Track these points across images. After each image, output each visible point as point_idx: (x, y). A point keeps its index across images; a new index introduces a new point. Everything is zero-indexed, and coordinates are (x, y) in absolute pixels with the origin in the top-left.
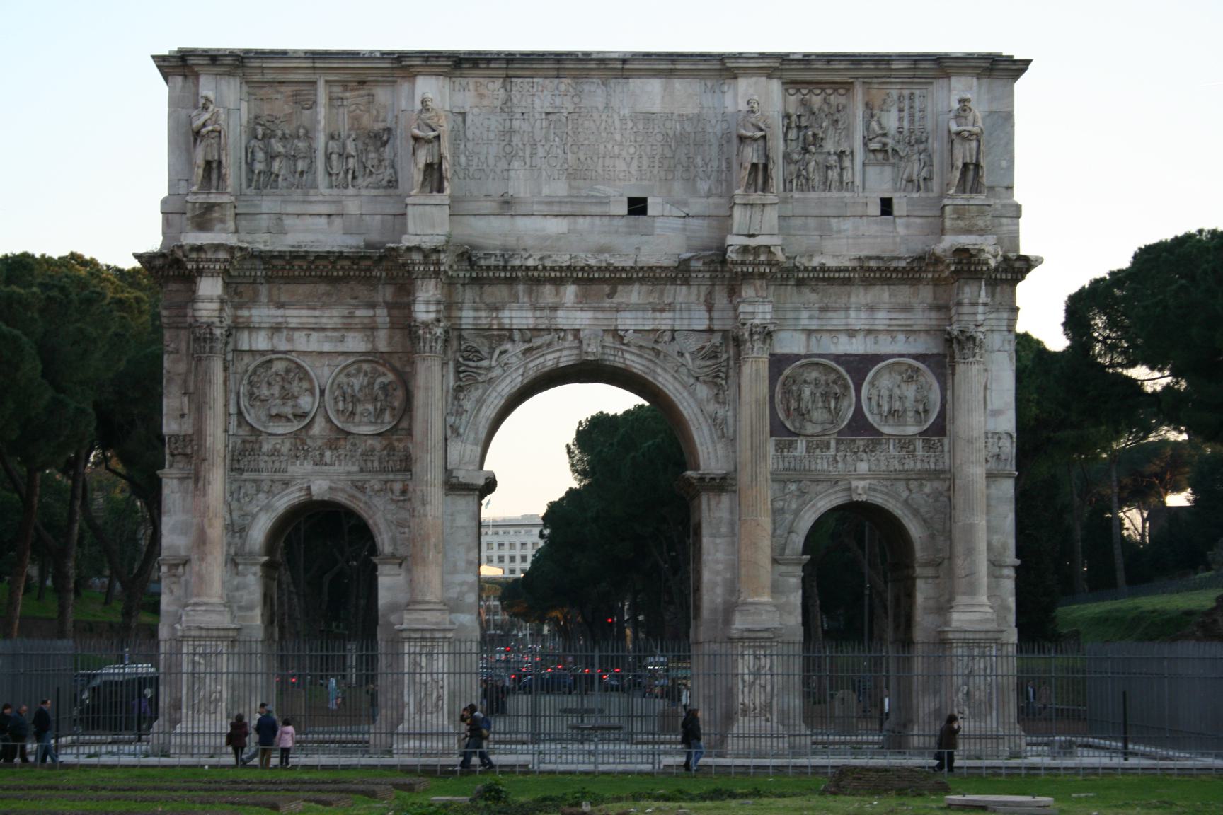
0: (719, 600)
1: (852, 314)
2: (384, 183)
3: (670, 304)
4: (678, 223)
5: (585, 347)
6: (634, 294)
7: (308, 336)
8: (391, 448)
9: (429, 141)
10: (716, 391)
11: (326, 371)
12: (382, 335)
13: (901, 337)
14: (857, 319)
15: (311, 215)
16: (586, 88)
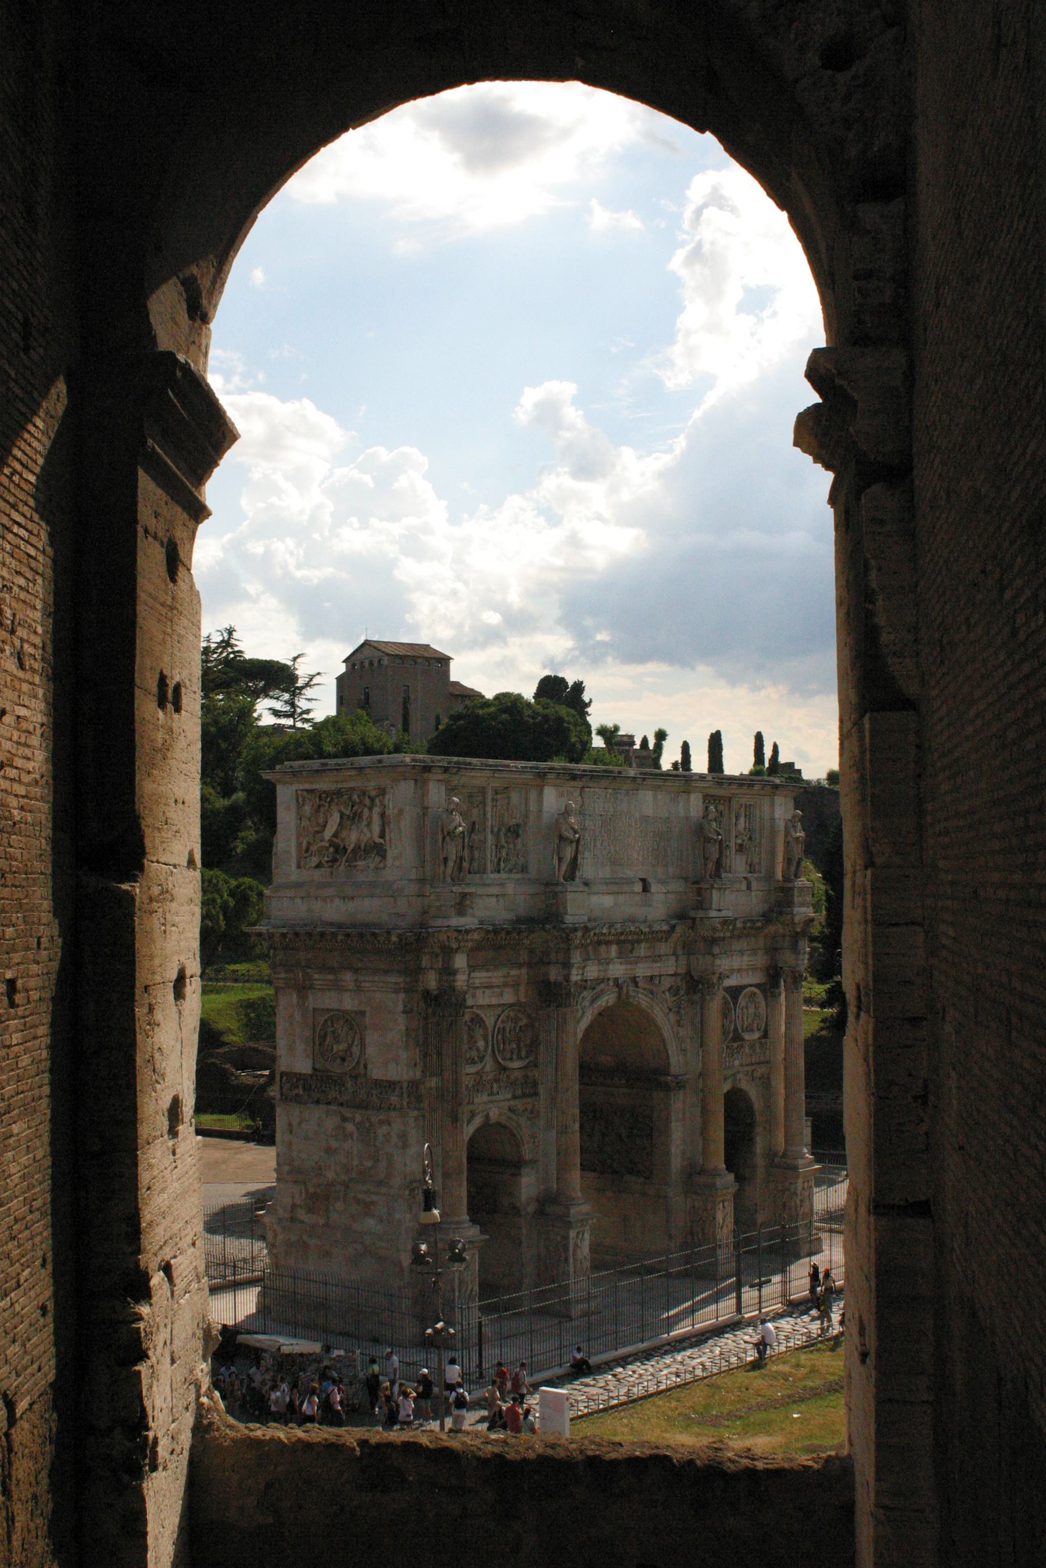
0: (679, 1166)
1: (734, 958)
2: (520, 869)
3: (659, 956)
4: (663, 896)
5: (625, 990)
6: (642, 950)
7: (484, 992)
8: (526, 1076)
9: (572, 842)
10: (679, 1018)
11: (493, 1020)
12: (522, 988)
13: (750, 973)
14: (736, 962)
15: (488, 895)
16: (619, 796)
